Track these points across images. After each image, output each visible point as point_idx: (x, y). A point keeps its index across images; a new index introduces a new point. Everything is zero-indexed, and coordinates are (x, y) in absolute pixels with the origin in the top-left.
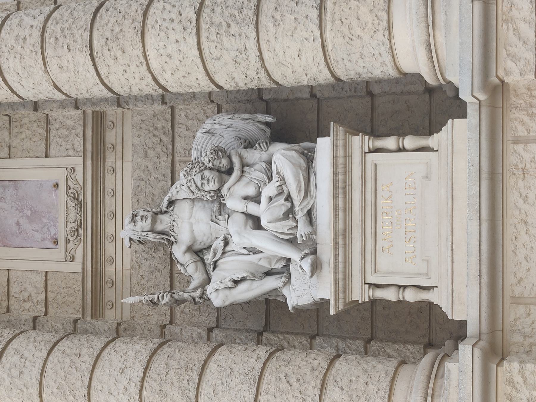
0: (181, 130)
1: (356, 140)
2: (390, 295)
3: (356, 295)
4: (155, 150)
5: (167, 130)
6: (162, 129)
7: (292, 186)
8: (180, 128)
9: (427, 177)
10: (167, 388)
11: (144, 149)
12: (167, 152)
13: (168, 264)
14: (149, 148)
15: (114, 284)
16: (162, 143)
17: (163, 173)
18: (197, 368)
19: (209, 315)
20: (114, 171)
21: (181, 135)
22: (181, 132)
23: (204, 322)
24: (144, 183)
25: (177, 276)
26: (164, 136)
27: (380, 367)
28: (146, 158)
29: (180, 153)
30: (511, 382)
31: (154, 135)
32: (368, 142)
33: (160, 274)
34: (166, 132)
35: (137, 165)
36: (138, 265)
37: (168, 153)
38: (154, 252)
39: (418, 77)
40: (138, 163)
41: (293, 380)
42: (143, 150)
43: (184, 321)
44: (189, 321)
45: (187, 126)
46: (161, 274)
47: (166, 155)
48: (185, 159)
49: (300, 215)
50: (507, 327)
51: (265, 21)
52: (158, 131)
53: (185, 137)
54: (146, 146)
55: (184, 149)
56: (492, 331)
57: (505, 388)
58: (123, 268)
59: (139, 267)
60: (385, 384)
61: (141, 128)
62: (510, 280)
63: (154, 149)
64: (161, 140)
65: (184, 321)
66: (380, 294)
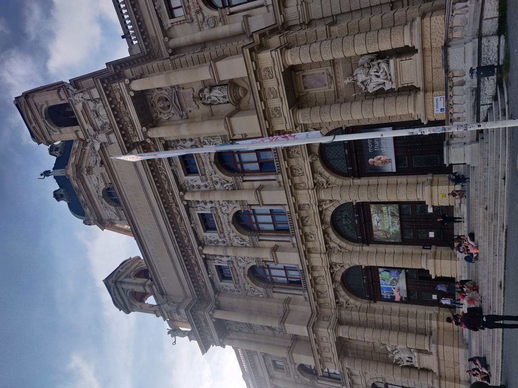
1: (398, 59)
2: (406, 85)
3: (400, 86)
7: (386, 70)
9: (411, 64)
10: (367, 109)
18: (372, 104)
27: (405, 97)
30: (428, 96)
32: (400, 60)
39: (408, 46)
41: (390, 103)
49: (388, 75)
50: (427, 87)
51: (379, 42)
56: (424, 88)
57: (427, 97)
60: (407, 100)
62: (427, 79)
66: (404, 85)
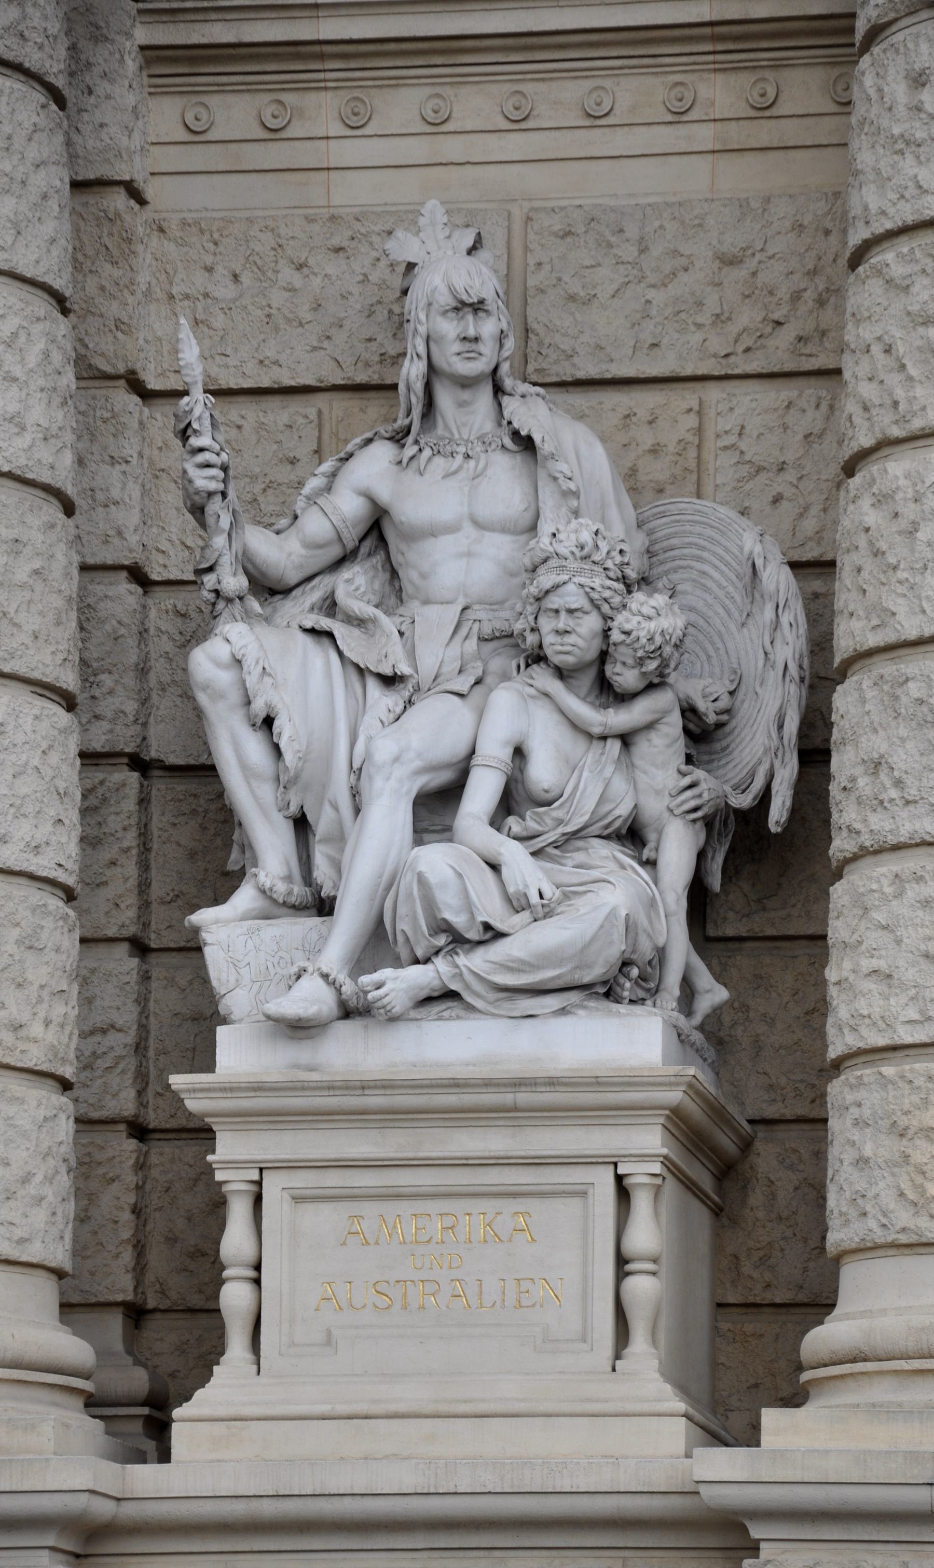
0: (810, 413)
4: (747, 301)
5: (814, 351)
6: (816, 330)
8: (818, 406)
11: (749, 252)
12: (737, 355)
13: (349, 378)
14: (754, 274)
15: (274, 133)
16: (769, 329)
17: (665, 341)
19: (188, 547)
20: (679, 116)
21: (792, 411)
22: (804, 411)
23: (163, 528)
24: (630, 260)
25: (311, 417)
26: (791, 339)
28: (718, 261)
29: (731, 409)
31: (796, 296)
33: (315, 344)
34: (806, 343)
35: (696, 222)
36: (345, 244)
37: (732, 359)
38: (390, 312)
40: (700, 225)
42: (748, 247)
43: (160, 449)
44: (163, 470)
45: (820, 436)
46: (315, 349)
47: (723, 353)
48: (709, 434)
52: (811, 312)
53: (785, 427)
54: (760, 262)
55: (743, 427)
58: (332, 173)
59: (338, 250)
61: (827, 233)
63: (748, 296)
64: (778, 323)
65: (160, 449)
